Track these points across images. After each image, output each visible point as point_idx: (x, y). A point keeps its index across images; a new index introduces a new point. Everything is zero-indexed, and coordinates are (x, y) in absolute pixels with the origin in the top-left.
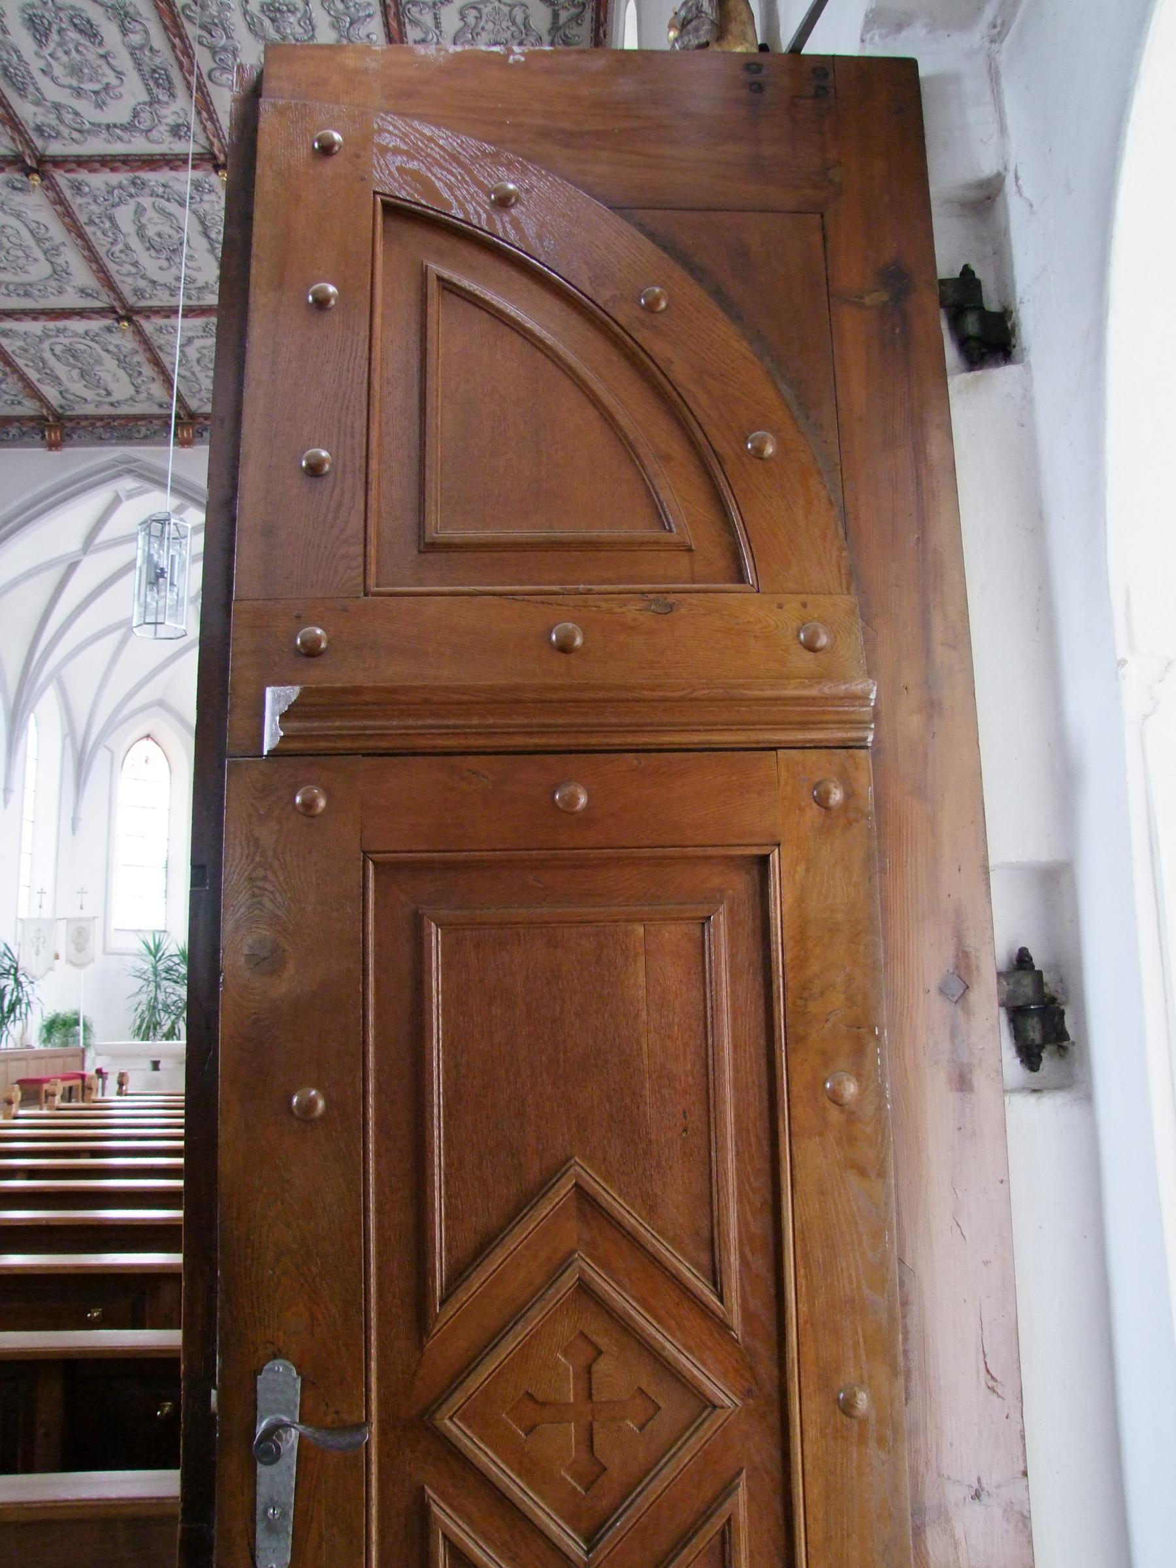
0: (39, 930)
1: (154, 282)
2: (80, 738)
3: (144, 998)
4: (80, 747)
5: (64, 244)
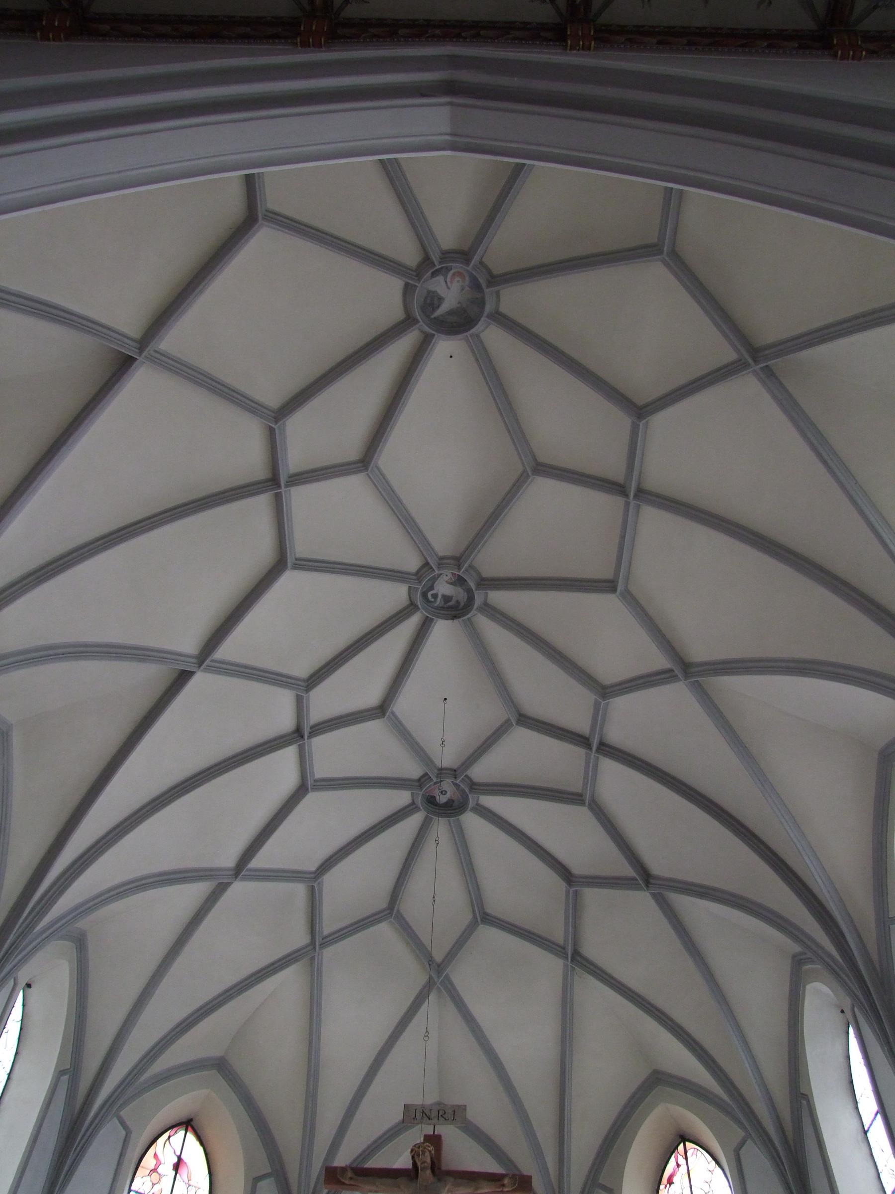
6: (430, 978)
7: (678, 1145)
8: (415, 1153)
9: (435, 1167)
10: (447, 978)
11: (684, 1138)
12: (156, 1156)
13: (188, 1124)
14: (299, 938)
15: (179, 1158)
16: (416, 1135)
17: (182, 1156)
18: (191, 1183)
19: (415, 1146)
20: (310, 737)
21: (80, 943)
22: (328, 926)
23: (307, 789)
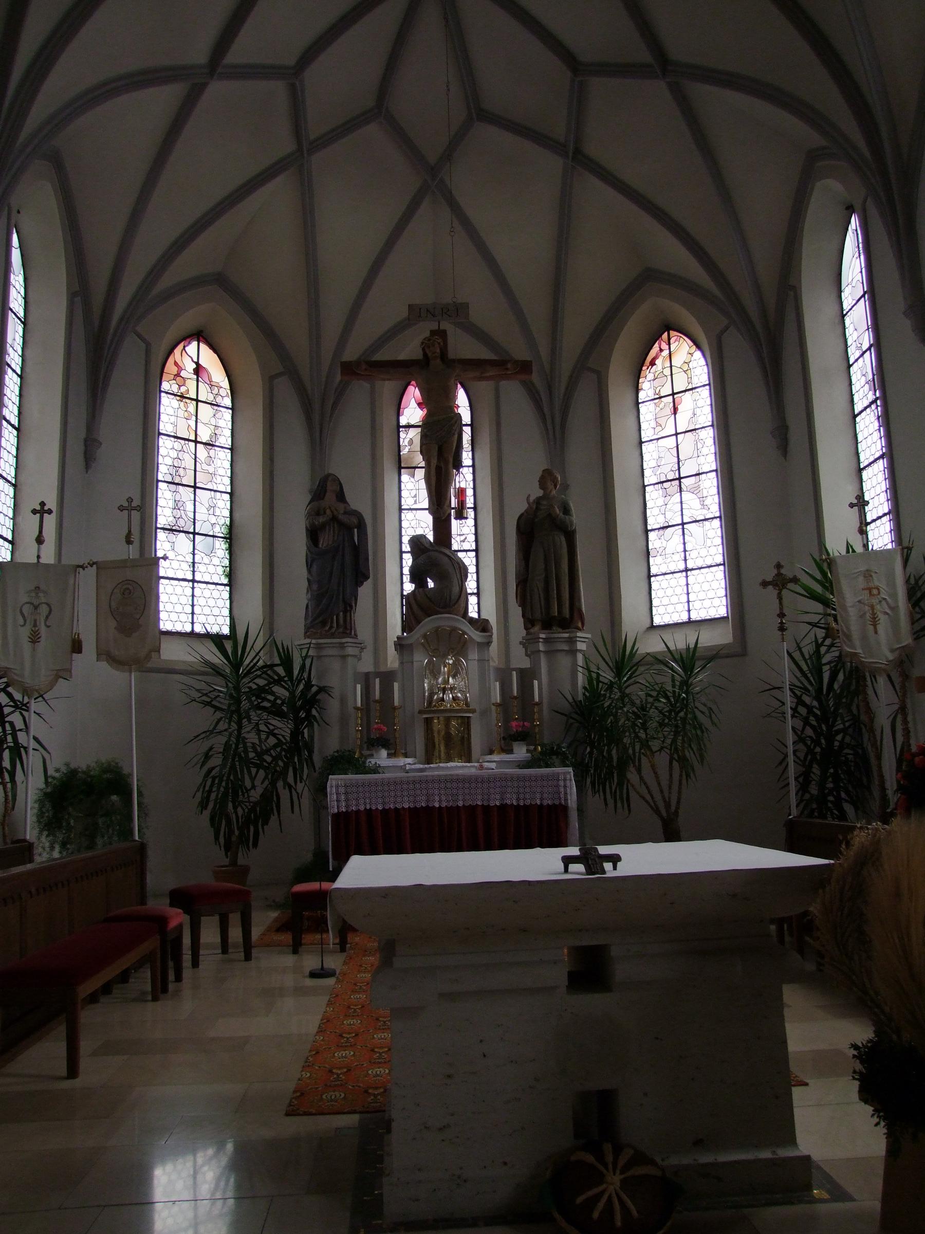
0: (37, 588)
2: (98, 299)
3: (219, 741)
7: (663, 333)
8: (426, 345)
9: (443, 356)
11: (668, 327)
12: (176, 364)
13: (199, 335)
14: (284, 145)
15: (197, 363)
16: (423, 330)
17: (200, 363)
18: (212, 383)
19: (425, 339)
21: (57, 162)
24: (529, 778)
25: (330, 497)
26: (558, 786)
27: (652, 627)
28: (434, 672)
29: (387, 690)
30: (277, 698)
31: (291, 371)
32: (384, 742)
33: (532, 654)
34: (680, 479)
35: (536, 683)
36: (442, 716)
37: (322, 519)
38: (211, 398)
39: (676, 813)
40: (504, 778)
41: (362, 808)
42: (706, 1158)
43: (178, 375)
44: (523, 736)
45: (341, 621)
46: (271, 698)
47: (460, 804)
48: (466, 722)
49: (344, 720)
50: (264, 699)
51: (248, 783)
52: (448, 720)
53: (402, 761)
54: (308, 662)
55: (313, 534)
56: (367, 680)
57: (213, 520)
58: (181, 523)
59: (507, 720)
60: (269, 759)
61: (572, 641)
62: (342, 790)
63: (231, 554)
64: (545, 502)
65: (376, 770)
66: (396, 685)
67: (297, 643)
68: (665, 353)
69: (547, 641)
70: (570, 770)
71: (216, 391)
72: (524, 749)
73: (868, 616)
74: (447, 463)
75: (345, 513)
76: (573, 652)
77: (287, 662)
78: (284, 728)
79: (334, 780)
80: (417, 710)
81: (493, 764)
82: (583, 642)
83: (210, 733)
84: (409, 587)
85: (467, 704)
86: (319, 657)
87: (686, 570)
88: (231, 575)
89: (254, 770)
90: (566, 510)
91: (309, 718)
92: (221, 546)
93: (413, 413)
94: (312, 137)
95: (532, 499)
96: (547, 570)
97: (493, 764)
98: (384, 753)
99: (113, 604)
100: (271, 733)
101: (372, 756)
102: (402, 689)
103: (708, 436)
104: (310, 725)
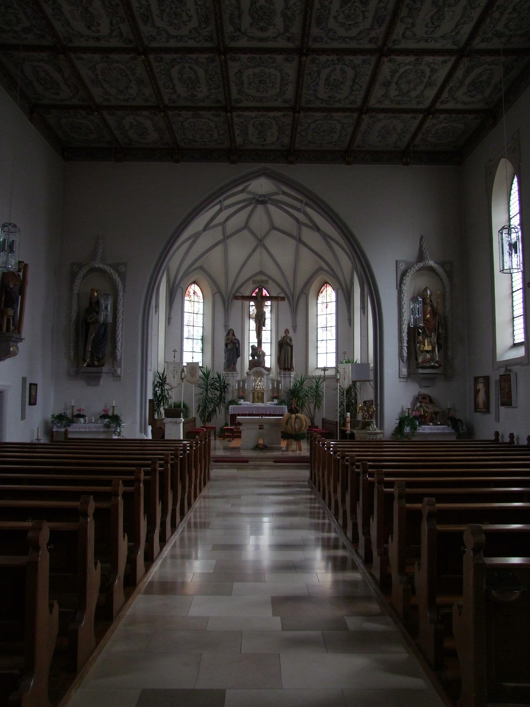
1: (317, 98)
4: (171, 286)
5: (291, 82)
6: (258, 243)
10: (263, 243)
11: (326, 283)
12: (189, 292)
13: (195, 282)
14: (221, 237)
15: (194, 291)
20: (223, 201)
22: (228, 233)
23: (222, 210)
24: (277, 408)
25: (231, 335)
26: (283, 410)
27: (317, 368)
28: (255, 381)
29: (244, 385)
30: (216, 386)
31: (220, 292)
32: (243, 398)
33: (281, 377)
34: (327, 327)
35: (280, 384)
36: (257, 392)
37: (228, 341)
38: (197, 300)
39: (314, 418)
40: (270, 408)
41: (237, 413)
42: (272, 446)
43: (189, 295)
44: (276, 398)
45: (233, 367)
46: (215, 386)
47: (260, 413)
48: (263, 394)
49: (233, 392)
50: (214, 386)
51: (210, 406)
52: (258, 393)
53: (247, 402)
54: (225, 377)
55: (226, 345)
56: (239, 382)
57: (198, 335)
58: (190, 336)
59: (273, 393)
60: (214, 401)
61: (290, 374)
62: (232, 409)
63: (202, 344)
64: (285, 338)
65: (240, 404)
66: (246, 384)
67: (222, 372)
68: (325, 290)
69: (284, 374)
70: (286, 406)
71: (199, 298)
72: (277, 401)
73: (344, 377)
74: (261, 325)
75: (234, 340)
76: (290, 377)
77: (219, 377)
78: (218, 393)
79: (231, 407)
80: (251, 390)
81: (269, 404)
82: (293, 374)
83: (202, 394)
84: (251, 358)
85: (263, 389)
86: (227, 376)
87: (327, 353)
88: (202, 350)
89: (211, 403)
90: (291, 340)
91: (224, 391)
92: (200, 342)
93: (253, 310)
94: (228, 235)
95: (282, 337)
96: (285, 356)
97: (269, 404)
98: (242, 400)
99: (190, 371)
100: (215, 395)
101: (239, 401)
102: (247, 384)
103: (334, 316)
104: (225, 393)
